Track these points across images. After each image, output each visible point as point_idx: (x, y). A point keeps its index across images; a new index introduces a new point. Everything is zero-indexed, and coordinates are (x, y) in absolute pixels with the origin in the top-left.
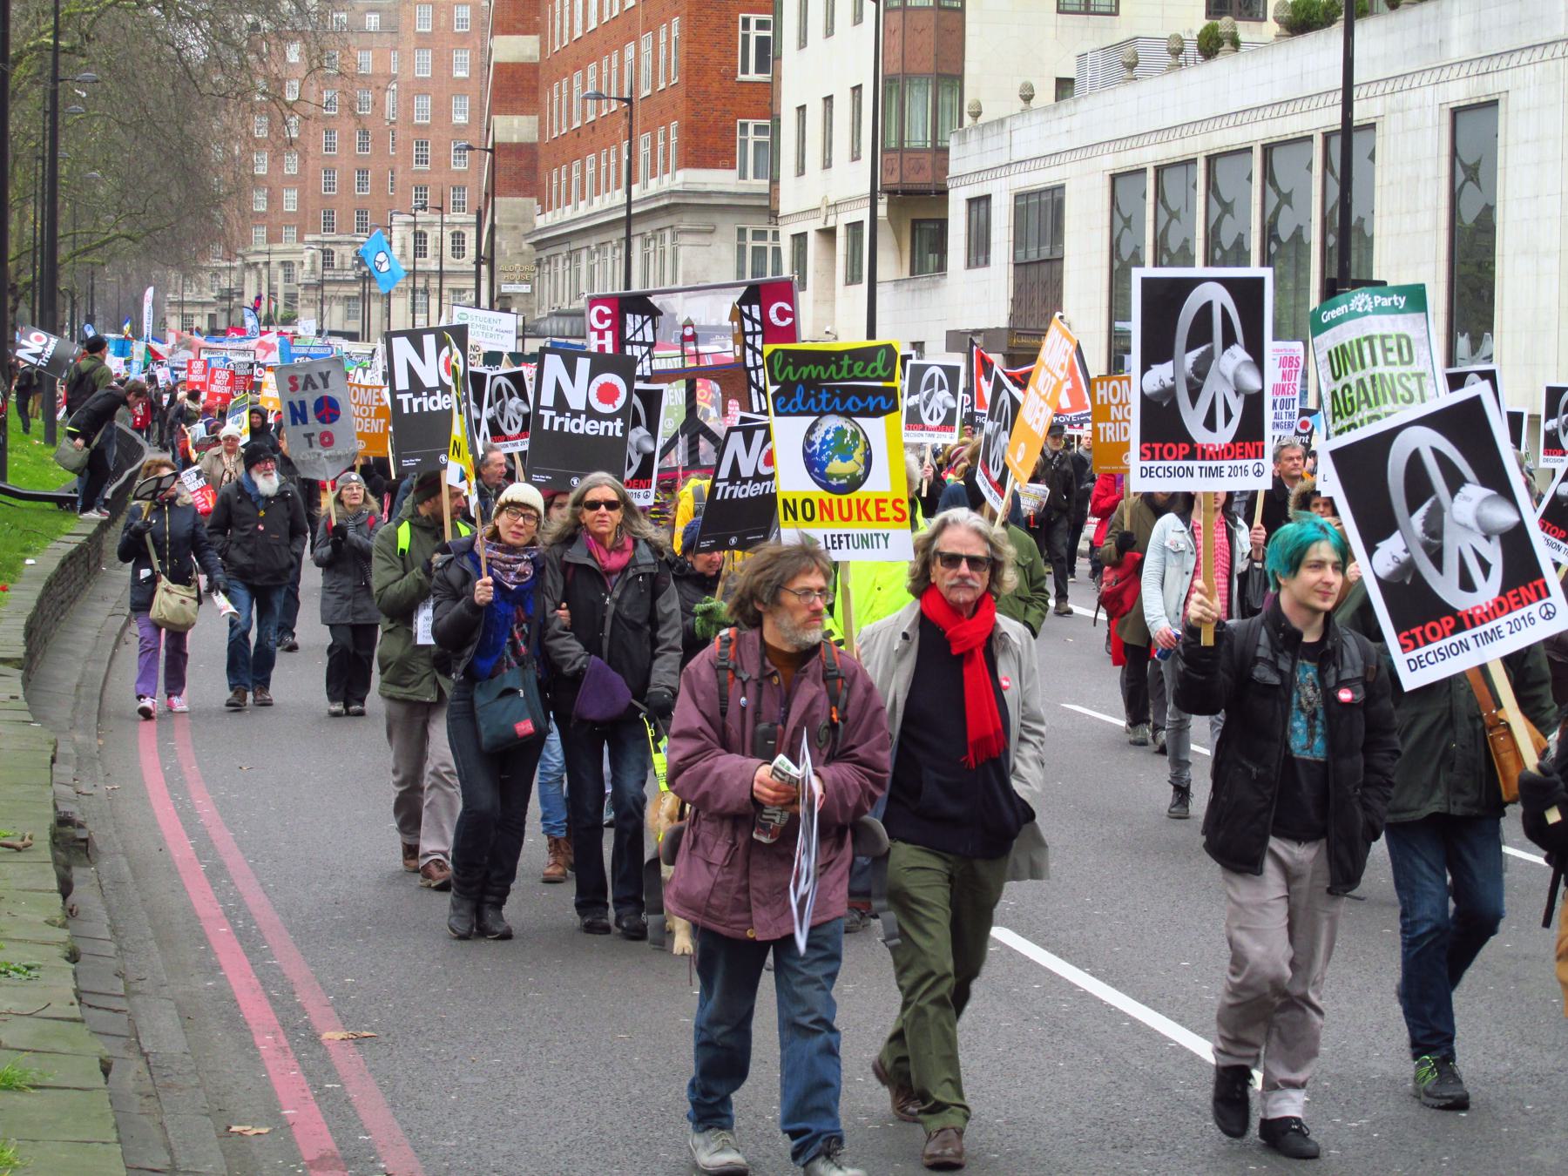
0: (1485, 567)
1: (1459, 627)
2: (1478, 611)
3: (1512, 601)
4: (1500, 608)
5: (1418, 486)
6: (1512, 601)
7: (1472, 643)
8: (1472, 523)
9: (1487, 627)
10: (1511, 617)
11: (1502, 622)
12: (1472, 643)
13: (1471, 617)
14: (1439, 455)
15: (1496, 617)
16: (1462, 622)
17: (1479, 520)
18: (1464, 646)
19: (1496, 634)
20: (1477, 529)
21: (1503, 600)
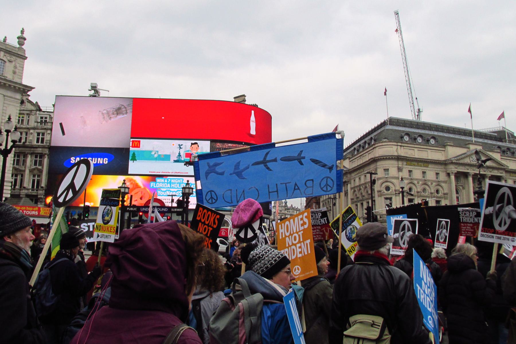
1: (494, 233)
4: (503, 233)
7: (495, 237)
8: (507, 212)
9: (499, 236)
11: (502, 236)
13: (498, 232)
14: (508, 195)
16: (495, 232)
18: (493, 237)
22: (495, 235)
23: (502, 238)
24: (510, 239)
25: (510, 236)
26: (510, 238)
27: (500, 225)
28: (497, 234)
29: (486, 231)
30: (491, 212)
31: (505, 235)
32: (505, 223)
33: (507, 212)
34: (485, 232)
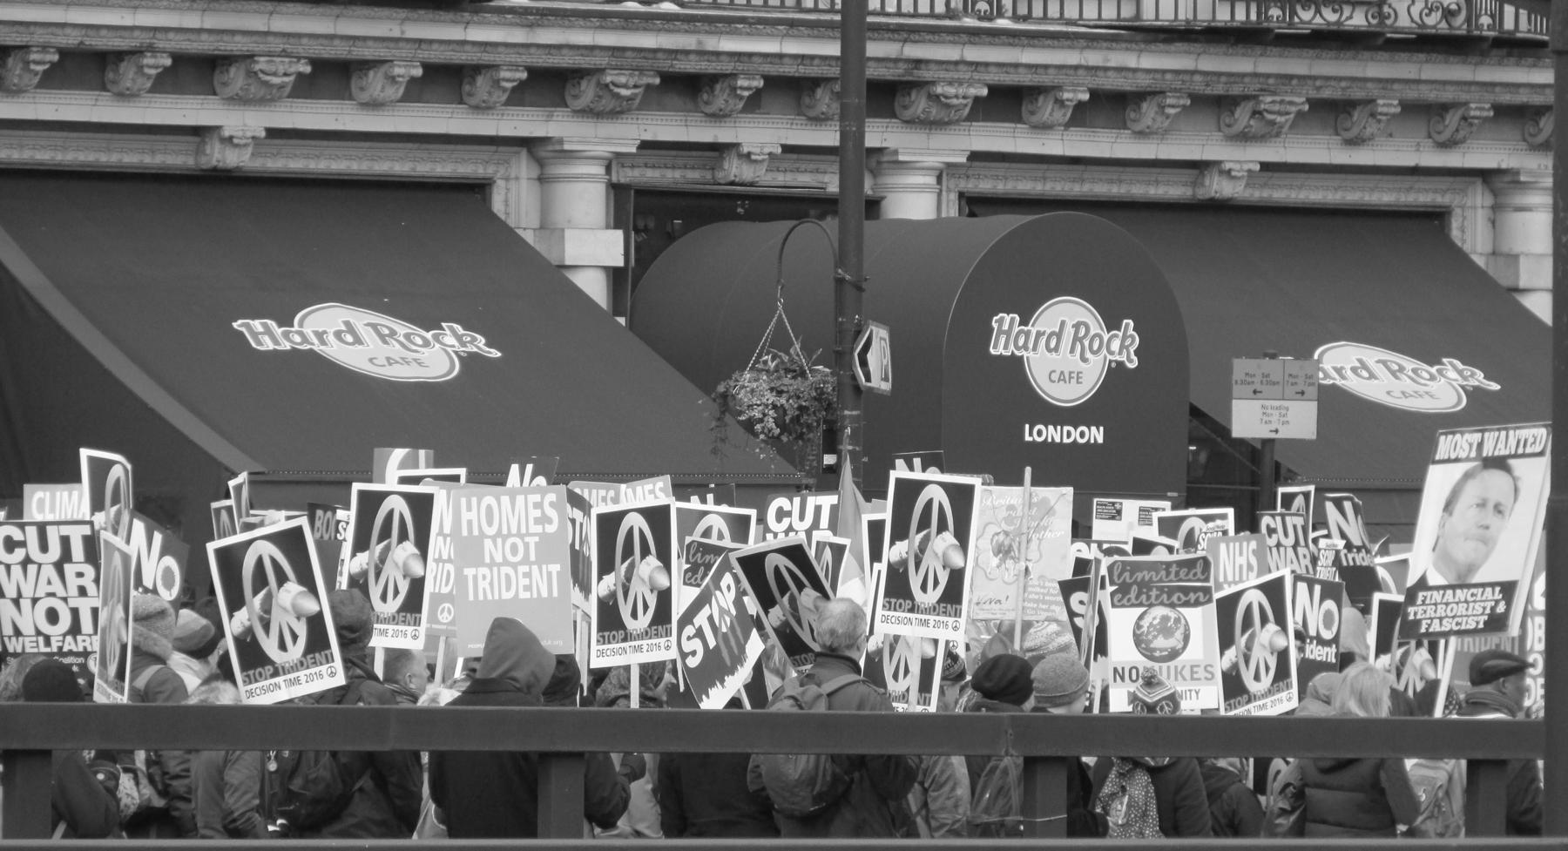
0: (295, 637)
1: (276, 674)
2: (287, 665)
3: (310, 661)
5: (260, 580)
6: (310, 661)
7: (283, 685)
8: (288, 605)
10: (307, 672)
11: (302, 674)
12: (283, 685)
15: (298, 670)
17: (294, 606)
18: (278, 686)
19: (297, 681)
20: (292, 612)
21: (303, 659)
22: (279, 680)
23: (303, 679)
24: (324, 673)
25: (321, 664)
26: (324, 668)
27: (283, 646)
28: (284, 674)
29: (252, 677)
30: (247, 624)
31: (308, 668)
32: (295, 637)
33: (288, 605)
34: (250, 683)
